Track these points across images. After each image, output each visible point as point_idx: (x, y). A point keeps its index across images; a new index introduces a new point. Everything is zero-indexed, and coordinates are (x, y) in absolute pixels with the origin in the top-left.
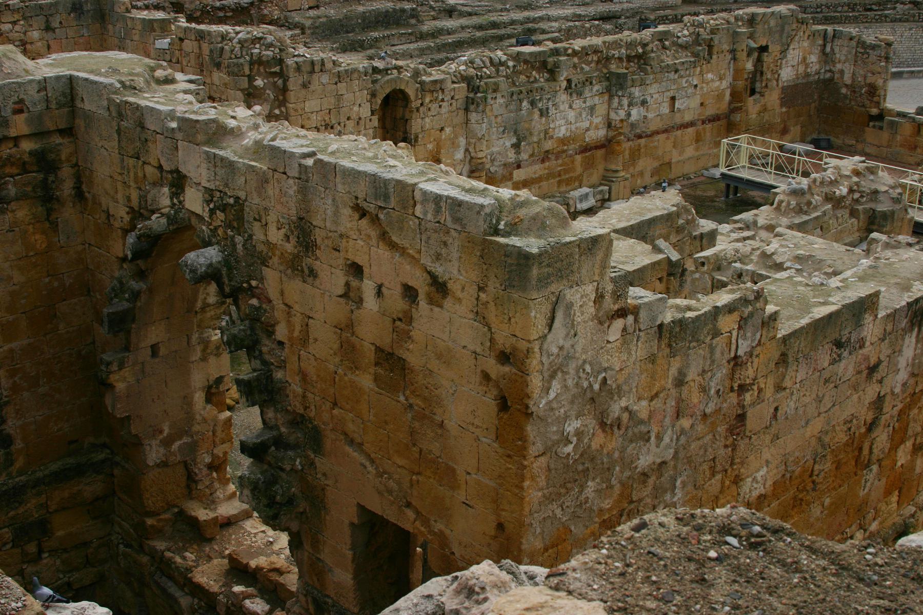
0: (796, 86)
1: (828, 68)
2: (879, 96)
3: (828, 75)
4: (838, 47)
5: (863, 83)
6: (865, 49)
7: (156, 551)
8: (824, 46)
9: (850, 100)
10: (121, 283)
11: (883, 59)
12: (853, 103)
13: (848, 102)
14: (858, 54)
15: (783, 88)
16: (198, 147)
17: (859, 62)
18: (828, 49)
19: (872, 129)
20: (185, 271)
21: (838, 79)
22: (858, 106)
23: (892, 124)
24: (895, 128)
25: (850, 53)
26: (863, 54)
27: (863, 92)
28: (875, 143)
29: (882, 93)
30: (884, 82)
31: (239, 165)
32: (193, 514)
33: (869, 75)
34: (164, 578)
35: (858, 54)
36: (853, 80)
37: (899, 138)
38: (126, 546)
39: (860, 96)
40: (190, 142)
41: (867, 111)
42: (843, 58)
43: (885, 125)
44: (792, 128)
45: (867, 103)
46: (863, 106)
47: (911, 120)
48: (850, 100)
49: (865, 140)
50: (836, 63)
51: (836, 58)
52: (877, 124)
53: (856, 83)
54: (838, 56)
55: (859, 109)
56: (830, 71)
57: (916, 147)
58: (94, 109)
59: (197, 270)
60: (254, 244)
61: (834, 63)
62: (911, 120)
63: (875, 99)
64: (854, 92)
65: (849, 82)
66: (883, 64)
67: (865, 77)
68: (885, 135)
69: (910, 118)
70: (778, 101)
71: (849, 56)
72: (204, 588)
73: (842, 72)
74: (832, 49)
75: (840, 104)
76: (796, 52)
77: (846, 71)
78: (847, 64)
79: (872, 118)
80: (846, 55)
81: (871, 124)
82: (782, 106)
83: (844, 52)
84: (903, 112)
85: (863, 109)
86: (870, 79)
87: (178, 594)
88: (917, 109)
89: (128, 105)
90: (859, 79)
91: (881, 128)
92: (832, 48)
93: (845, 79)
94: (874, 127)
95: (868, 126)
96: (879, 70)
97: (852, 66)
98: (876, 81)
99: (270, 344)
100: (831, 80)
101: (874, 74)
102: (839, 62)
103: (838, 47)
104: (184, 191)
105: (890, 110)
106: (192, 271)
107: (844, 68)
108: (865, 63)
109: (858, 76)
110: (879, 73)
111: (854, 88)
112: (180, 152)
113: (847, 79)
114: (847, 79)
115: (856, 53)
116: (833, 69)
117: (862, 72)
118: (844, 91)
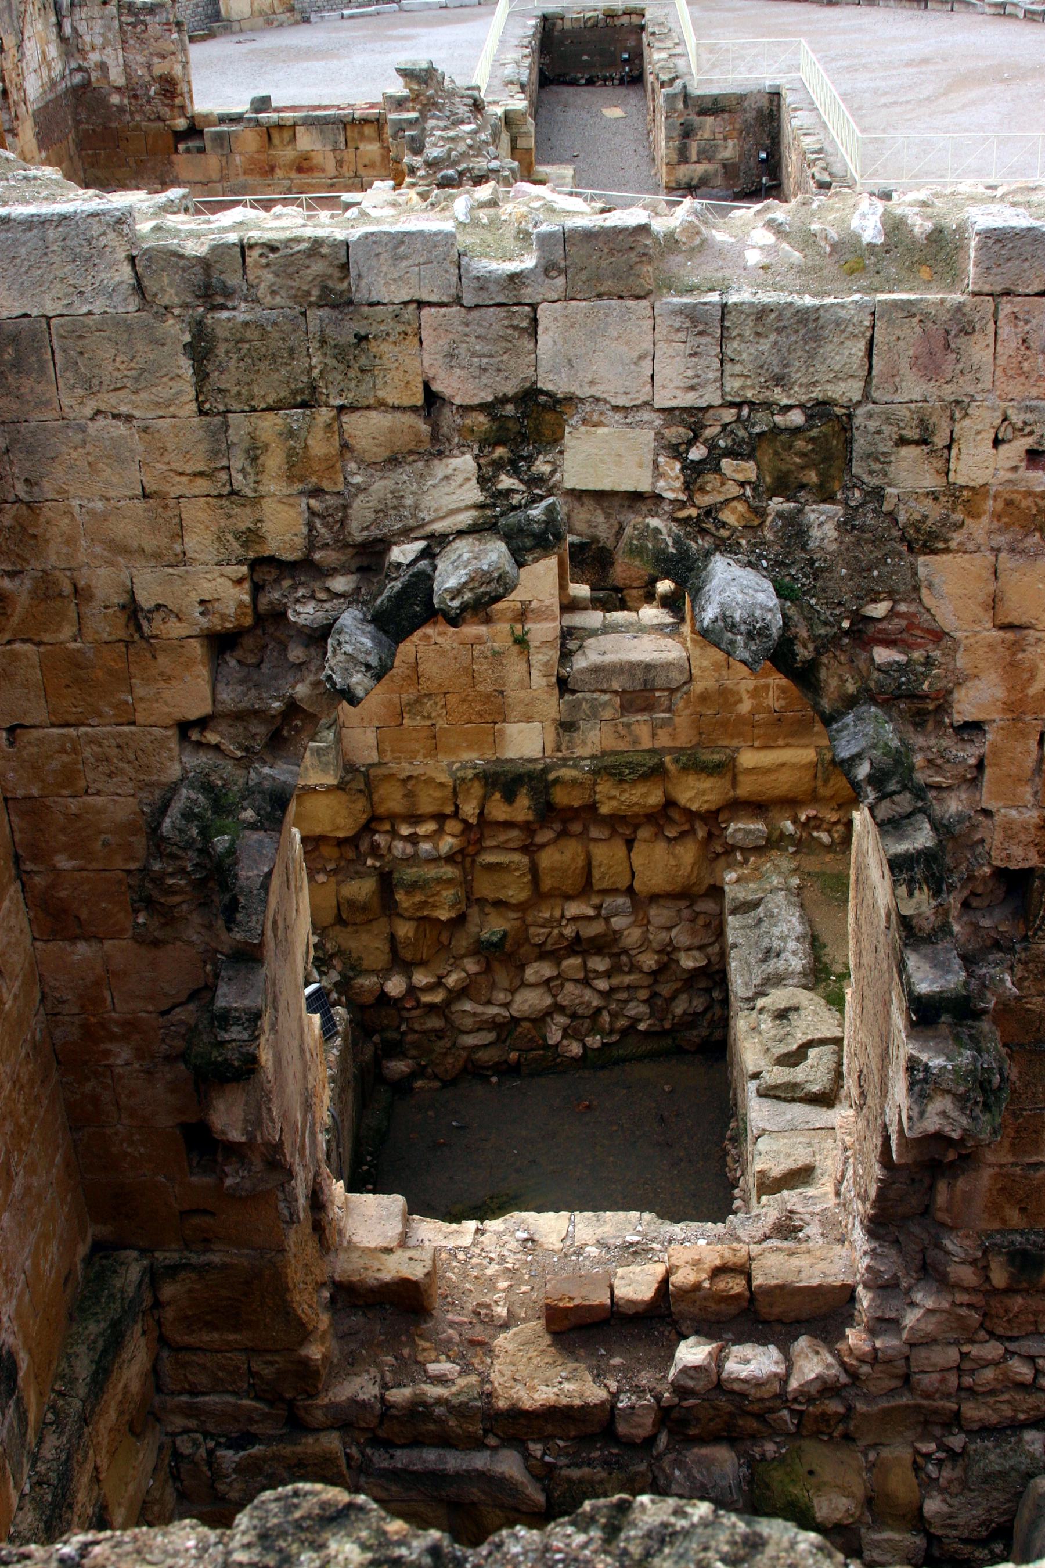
0: (46, 106)
1: (74, 65)
2: (181, 95)
3: (78, 78)
4: (84, 23)
5: (147, 79)
6: (136, 15)
7: (363, 1405)
8: (59, 25)
9: (132, 113)
10: (207, 788)
11: (174, 29)
12: (138, 118)
13: (128, 117)
14: (125, 27)
15: (34, 112)
16: (645, 303)
17: (131, 42)
18: (68, 30)
19: (185, 156)
20: (732, 642)
21: (98, 80)
22: (149, 120)
23: (219, 137)
24: (226, 143)
25: (110, 28)
26: (134, 25)
27: (152, 93)
28: (197, 179)
29: (185, 89)
30: (184, 67)
31: (843, 313)
32: (387, 1276)
33: (156, 60)
34: (398, 1453)
35: (125, 27)
36: (128, 77)
37: (238, 159)
38: (238, 1443)
39: (148, 102)
40: (599, 296)
41: (169, 126)
42: (98, 41)
43: (208, 144)
45: (165, 111)
46: (159, 118)
47: (252, 124)
48: (132, 113)
49: (177, 178)
50: (87, 53)
51: (84, 43)
52: (190, 144)
53: (135, 80)
54: (87, 38)
55: (152, 125)
56: (80, 69)
57: (272, 169)
58: (51, 308)
59: (767, 627)
60: (887, 507)
61: (83, 53)
62: (252, 124)
63: (178, 101)
64: (136, 97)
65: (121, 81)
66: (175, 36)
67: (149, 66)
68: (213, 161)
69: (250, 120)
70: (34, 141)
71: (110, 35)
72: (570, 1408)
73: (103, 66)
74: (75, 29)
75: (114, 125)
76: (33, 42)
77: (111, 63)
78: (109, 50)
79: (180, 136)
80: (102, 35)
81: (181, 147)
82: (40, 148)
83: (97, 29)
84: (228, 115)
85: (161, 124)
86: (160, 68)
87: (480, 1461)
88: (252, 103)
89: (255, 253)
90: (140, 73)
91: (201, 150)
93: (112, 78)
94: (188, 151)
95: (176, 151)
96: (172, 47)
97: (120, 53)
98: (172, 68)
99: (933, 741)
100: (86, 85)
101: (164, 57)
102: (93, 49)
103: (84, 23)
104: (557, 439)
105: (206, 116)
106: (750, 636)
107: (105, 59)
108: (142, 41)
109: (134, 67)
110: (174, 54)
111: (133, 89)
112: (544, 338)
113: (116, 76)
114: (116, 76)
115: (121, 27)
116: (85, 64)
117: (140, 59)
118: (115, 99)
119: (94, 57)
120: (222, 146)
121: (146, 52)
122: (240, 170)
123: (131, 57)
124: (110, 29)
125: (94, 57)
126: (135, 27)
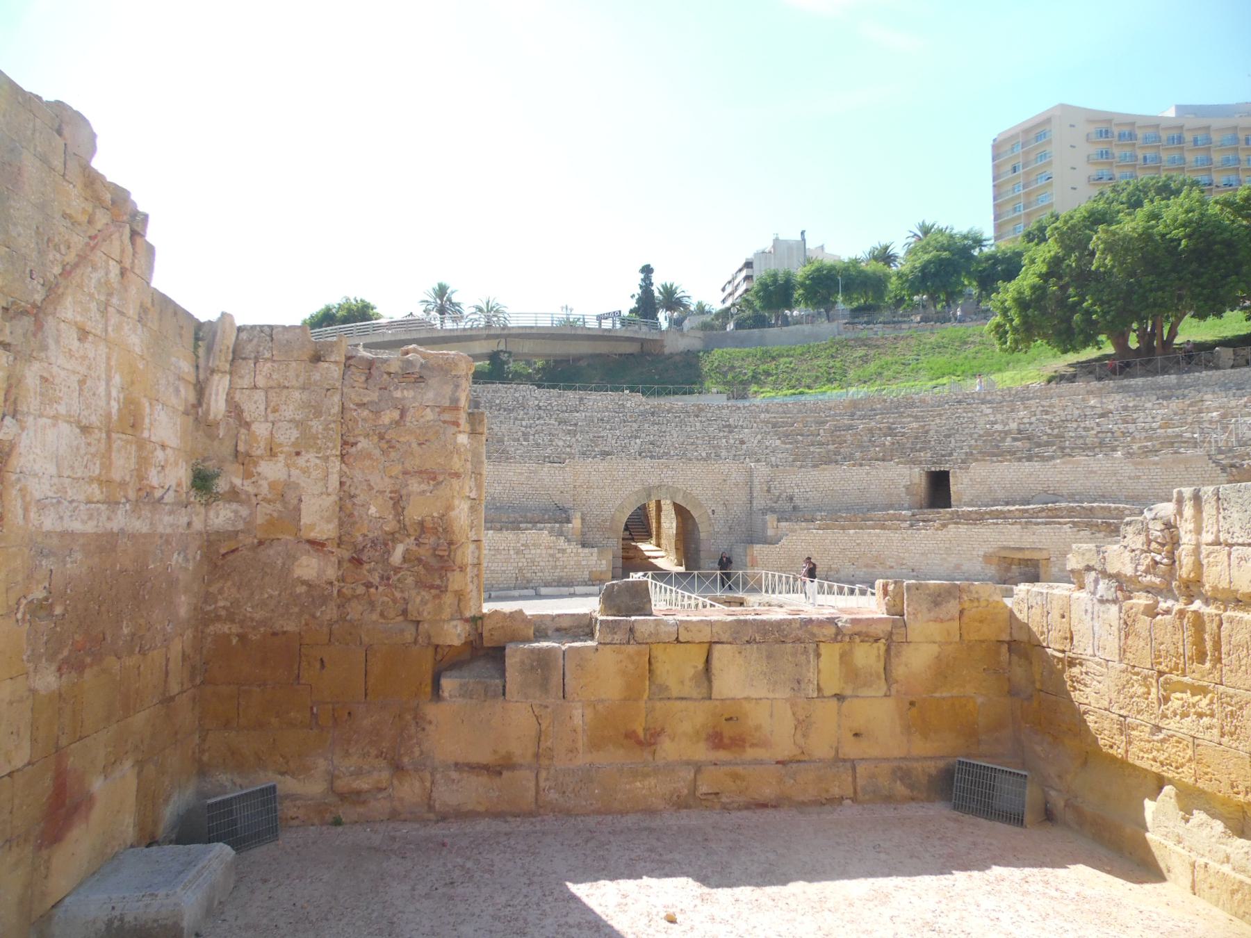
4: (259, 395)
17: (363, 444)
18: (217, 405)
23: (543, 661)
24: (556, 679)
27: (397, 556)
33: (415, 486)
42: (287, 436)
43: (512, 674)
44: (97, 785)
54: (261, 430)
65: (326, 530)
67: (398, 502)
71: (316, 426)
74: (235, 409)
78: (310, 458)
80: (298, 424)
92: (230, 399)
97: (336, 466)
98: (450, 508)
102: (272, 453)
103: (259, 395)
117: (380, 482)
119: (272, 471)
120: (544, 685)
121: (396, 470)
122: (581, 741)
123: (358, 475)
124: (318, 413)
125: (272, 471)
126: (377, 413)
